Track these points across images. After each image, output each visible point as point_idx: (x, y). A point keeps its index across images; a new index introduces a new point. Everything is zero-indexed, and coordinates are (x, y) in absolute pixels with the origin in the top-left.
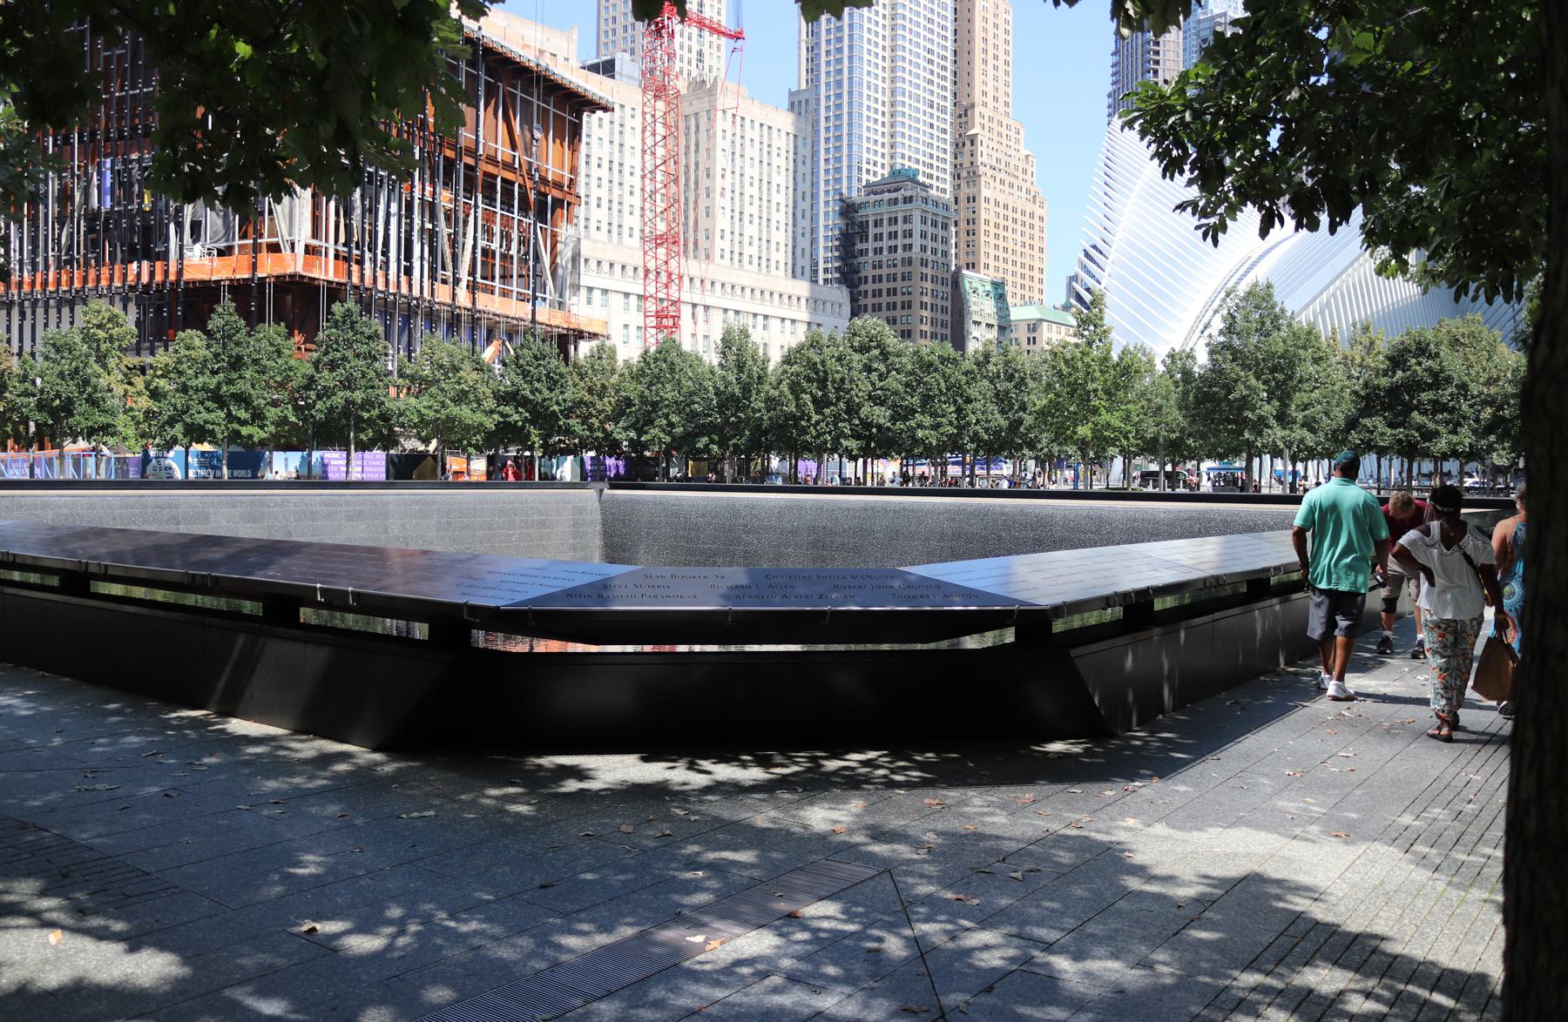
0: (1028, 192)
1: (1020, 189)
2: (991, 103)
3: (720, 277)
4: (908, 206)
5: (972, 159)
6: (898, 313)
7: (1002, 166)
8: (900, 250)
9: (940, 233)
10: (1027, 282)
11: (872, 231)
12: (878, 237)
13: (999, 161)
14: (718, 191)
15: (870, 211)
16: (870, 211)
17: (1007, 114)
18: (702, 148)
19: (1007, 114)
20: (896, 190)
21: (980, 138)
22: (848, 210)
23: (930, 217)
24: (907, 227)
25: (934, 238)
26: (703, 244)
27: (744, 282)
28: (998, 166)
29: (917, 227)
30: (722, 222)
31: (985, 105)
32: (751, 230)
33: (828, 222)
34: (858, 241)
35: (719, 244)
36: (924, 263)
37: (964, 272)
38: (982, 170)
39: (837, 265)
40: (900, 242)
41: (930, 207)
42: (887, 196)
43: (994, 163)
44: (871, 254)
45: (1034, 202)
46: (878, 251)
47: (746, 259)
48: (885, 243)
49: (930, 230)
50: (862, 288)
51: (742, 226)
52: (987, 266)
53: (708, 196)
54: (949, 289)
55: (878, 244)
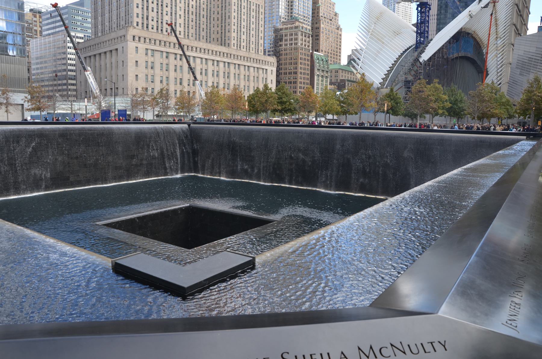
3: (234, 52)
4: (296, 30)
7: (328, 17)
8: (293, 45)
9: (307, 39)
10: (335, 56)
12: (286, 40)
14: (233, 24)
15: (283, 31)
18: (227, 9)
21: (320, 7)
22: (276, 31)
24: (296, 37)
26: (227, 42)
27: (241, 55)
28: (326, 17)
30: (234, 35)
33: (271, 35)
34: (279, 41)
35: (233, 42)
36: (302, 49)
37: (315, 52)
39: (272, 49)
40: (293, 42)
41: (304, 30)
43: (325, 16)
44: (284, 46)
46: (286, 45)
47: (242, 47)
48: (288, 42)
49: (304, 38)
50: (281, 57)
52: (322, 51)
54: (309, 58)
55: (286, 43)
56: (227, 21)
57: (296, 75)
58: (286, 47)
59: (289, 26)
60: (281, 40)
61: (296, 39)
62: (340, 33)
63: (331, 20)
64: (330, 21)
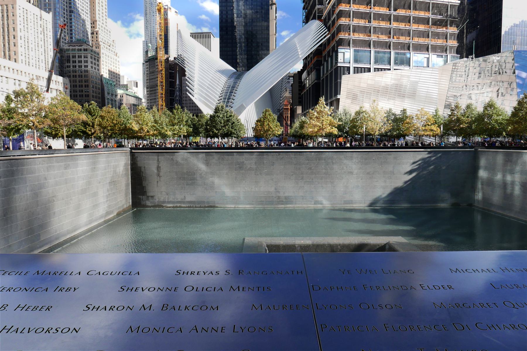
0: (114, 52)
1: (112, 51)
2: (101, 21)
4: (86, 52)
5: (97, 39)
6: (84, 88)
7: (106, 43)
11: (71, 59)
13: (105, 41)
16: (70, 52)
17: (106, 26)
19: (106, 26)
20: (81, 46)
23: (93, 57)
25: (95, 64)
28: (105, 42)
29: (89, 60)
31: (100, 21)
32: (32, 53)
38: (101, 43)
41: (93, 53)
42: (77, 47)
43: (104, 42)
44: (71, 67)
45: (116, 56)
49: (94, 61)
51: (29, 52)
53: (14, 38)
56: (12, 33)
57: (88, 98)
58: (74, 69)
59: (77, 47)
60: (69, 61)
61: (87, 62)
62: (118, 59)
63: (110, 46)
64: (108, 47)
